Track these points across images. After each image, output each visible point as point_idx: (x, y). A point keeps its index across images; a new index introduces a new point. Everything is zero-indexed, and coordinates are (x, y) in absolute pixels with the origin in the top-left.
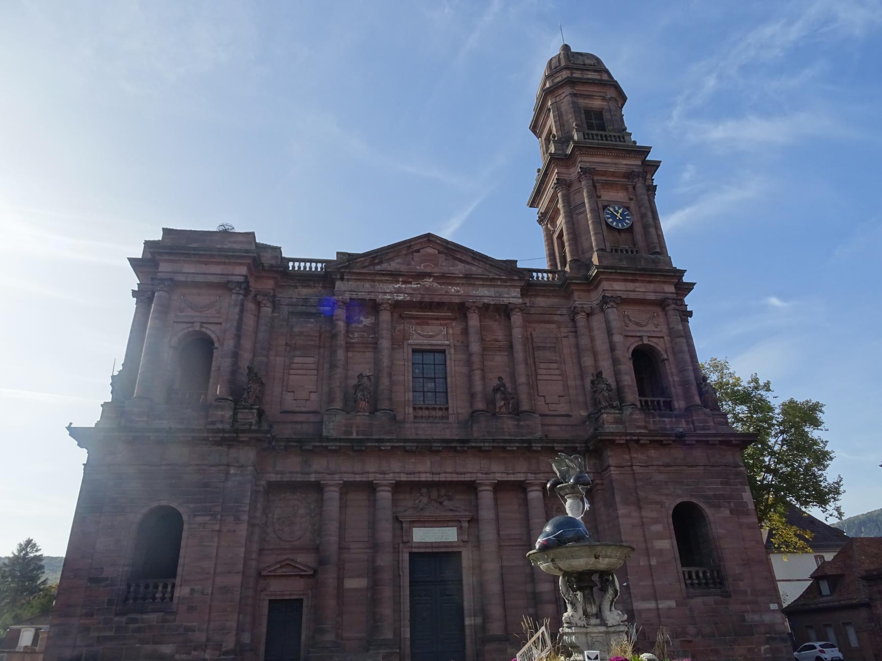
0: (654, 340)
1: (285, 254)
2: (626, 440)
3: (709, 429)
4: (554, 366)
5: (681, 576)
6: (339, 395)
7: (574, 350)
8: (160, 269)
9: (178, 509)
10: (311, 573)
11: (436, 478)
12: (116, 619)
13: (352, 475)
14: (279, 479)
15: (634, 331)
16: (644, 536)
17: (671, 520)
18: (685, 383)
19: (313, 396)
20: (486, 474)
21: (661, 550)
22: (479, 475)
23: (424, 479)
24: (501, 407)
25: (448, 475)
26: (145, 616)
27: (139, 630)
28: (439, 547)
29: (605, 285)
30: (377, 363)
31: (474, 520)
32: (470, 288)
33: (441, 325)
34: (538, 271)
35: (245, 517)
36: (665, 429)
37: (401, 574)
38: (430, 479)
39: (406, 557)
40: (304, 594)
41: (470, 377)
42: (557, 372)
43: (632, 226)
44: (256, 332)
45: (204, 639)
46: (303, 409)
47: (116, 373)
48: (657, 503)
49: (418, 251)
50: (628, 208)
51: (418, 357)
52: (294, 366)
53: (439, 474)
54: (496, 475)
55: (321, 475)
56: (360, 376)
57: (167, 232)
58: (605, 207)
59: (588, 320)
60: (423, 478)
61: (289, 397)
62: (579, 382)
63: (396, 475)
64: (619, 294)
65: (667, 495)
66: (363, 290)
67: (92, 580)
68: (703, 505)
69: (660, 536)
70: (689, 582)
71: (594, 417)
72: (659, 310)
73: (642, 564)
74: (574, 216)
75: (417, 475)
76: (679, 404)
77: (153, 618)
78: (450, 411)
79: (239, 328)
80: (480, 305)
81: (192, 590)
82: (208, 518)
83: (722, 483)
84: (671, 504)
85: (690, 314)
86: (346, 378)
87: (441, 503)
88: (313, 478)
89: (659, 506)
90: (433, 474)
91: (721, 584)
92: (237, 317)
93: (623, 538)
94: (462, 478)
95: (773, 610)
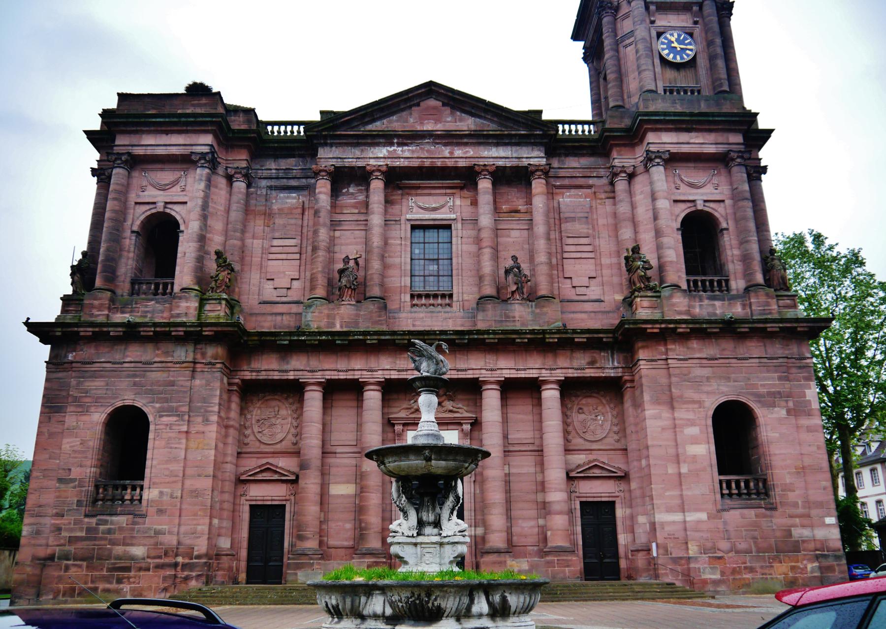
0: (712, 205)
1: (262, 116)
2: (660, 328)
3: (770, 313)
5: (717, 486)
6: (321, 281)
7: (611, 221)
8: (117, 143)
10: (294, 478)
12: (86, 520)
13: (336, 373)
14: (254, 377)
16: (676, 441)
17: (710, 422)
18: (746, 259)
19: (296, 284)
20: (492, 370)
21: (694, 457)
22: (483, 372)
24: (513, 293)
26: (114, 518)
27: (109, 531)
29: (651, 137)
30: (367, 242)
31: (476, 424)
32: (482, 148)
33: (446, 194)
34: (563, 122)
35: (215, 418)
36: (715, 314)
40: (286, 500)
41: (478, 255)
42: (589, 248)
43: (695, 57)
44: (228, 211)
45: (175, 543)
47: (75, 263)
48: (694, 402)
49: (418, 105)
50: (691, 35)
51: (419, 234)
52: (274, 250)
54: (504, 371)
55: (300, 373)
56: (346, 260)
57: (122, 97)
58: (659, 35)
59: (629, 183)
61: (269, 286)
63: (386, 372)
64: (668, 147)
65: (708, 393)
67: (60, 480)
68: (752, 405)
69: (695, 441)
70: (726, 491)
71: (629, 302)
72: (721, 167)
73: (670, 471)
74: (621, 49)
76: (737, 284)
77: (122, 520)
78: (455, 298)
79: (205, 206)
81: (161, 493)
82: (175, 419)
83: (780, 378)
84: (711, 403)
85: (764, 170)
86: (331, 261)
88: (291, 376)
89: (696, 406)
91: (767, 494)
92: (202, 194)
93: (650, 443)
94: (462, 375)
95: (829, 525)
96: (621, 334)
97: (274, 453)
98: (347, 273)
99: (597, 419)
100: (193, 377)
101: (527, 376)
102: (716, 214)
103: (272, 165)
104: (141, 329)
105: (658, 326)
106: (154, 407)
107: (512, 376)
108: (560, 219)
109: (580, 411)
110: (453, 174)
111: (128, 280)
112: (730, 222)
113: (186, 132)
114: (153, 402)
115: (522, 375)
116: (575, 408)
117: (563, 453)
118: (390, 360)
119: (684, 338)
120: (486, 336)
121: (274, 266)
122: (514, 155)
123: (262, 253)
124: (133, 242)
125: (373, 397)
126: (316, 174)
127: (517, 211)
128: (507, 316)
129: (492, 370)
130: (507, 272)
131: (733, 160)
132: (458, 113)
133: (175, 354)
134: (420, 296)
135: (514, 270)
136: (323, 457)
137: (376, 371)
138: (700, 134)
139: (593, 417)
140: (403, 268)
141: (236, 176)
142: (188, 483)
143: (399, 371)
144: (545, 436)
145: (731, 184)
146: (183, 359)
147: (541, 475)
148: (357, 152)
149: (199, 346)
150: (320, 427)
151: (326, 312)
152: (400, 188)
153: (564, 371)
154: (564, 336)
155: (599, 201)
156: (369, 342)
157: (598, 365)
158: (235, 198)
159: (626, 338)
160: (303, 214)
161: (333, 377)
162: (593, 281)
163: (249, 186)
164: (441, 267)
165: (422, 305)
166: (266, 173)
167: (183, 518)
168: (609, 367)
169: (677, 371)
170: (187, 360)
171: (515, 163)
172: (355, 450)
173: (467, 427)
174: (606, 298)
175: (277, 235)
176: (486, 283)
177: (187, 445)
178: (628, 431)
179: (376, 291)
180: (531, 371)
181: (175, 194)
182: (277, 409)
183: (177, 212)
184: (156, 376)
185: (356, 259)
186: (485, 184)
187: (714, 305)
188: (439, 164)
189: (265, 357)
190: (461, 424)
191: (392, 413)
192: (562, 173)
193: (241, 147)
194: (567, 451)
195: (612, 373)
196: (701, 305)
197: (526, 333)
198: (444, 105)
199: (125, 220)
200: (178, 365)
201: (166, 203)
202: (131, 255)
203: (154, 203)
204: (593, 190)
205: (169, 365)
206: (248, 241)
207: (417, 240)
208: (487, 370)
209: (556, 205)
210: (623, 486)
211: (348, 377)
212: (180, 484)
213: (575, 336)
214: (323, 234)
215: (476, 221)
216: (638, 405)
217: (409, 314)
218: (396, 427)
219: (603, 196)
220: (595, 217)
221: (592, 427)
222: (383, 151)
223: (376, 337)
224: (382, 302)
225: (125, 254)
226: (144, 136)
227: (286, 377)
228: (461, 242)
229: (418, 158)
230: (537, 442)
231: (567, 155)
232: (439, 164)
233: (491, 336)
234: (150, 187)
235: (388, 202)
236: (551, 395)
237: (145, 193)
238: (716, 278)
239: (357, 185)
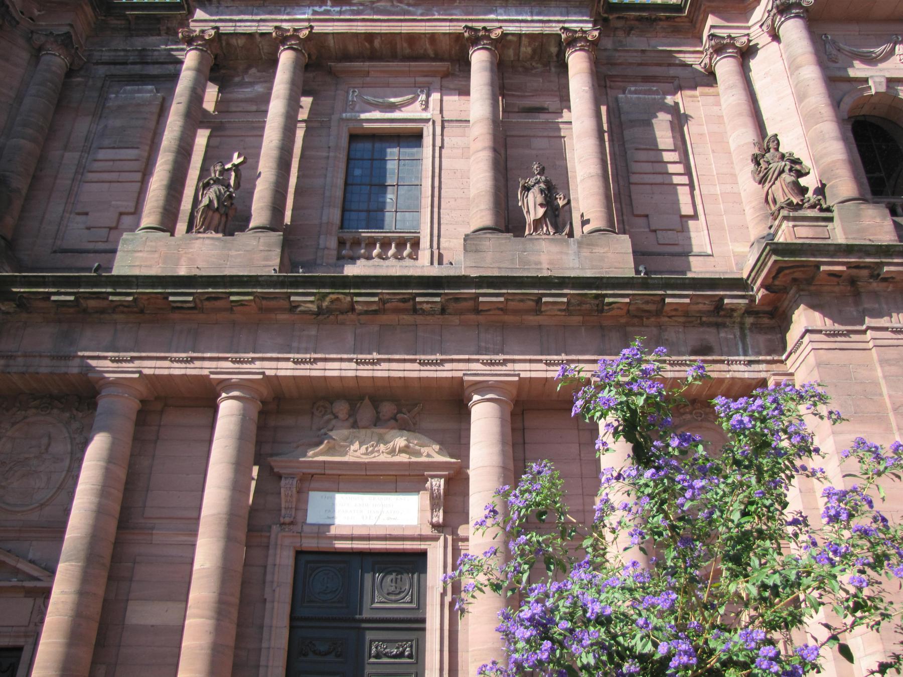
28: (369, 538)
37: (268, 596)
96: (763, 285)
107: (534, 375)
123: (76, 172)
140: (327, 194)
163: (70, 73)
166: (107, 56)
182: (45, 441)
207: (359, 155)
218: (283, 482)
227: (63, 370)
231: (629, 31)
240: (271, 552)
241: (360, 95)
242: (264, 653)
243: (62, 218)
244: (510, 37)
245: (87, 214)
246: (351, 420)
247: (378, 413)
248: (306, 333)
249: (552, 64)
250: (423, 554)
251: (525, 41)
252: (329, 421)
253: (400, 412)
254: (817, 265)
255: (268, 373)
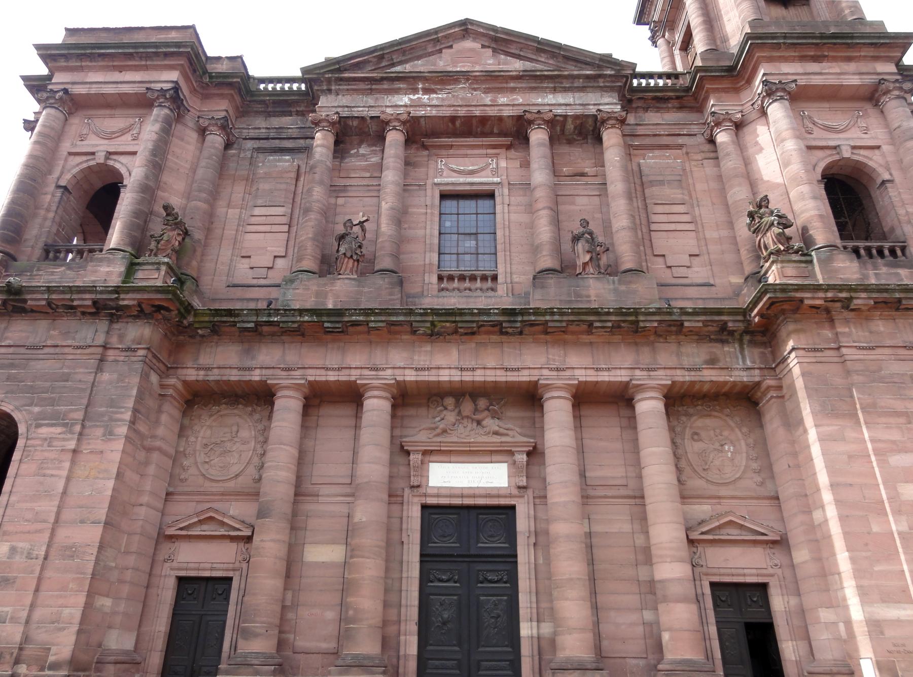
0: (862, 152)
4: (681, 209)
7: (714, 185)
9: (12, 414)
11: (468, 377)
13: (323, 372)
14: (200, 378)
15: (821, 139)
19: (280, 263)
20: (558, 370)
22: (546, 372)
23: (447, 379)
24: (585, 265)
25: (488, 372)
28: (474, 496)
31: (535, 453)
33: (487, 155)
35: (123, 430)
37: (405, 539)
38: (457, 379)
39: (414, 514)
44: (194, 170)
45: (18, 638)
46: (262, 282)
49: (451, 47)
51: (451, 205)
52: (254, 220)
53: (473, 369)
54: (577, 372)
55: (270, 372)
59: (737, 135)
60: (445, 376)
61: (244, 265)
62: (725, 233)
63: (397, 372)
66: (362, 105)
72: (868, 106)
75: (433, 372)
78: (500, 279)
80: (548, 116)
81: (13, 550)
82: (59, 430)
87: (479, 423)
88: (256, 376)
90: (462, 369)
94: (512, 377)
96: (760, 314)
97: (222, 494)
98: (348, 239)
99: (725, 447)
100: (99, 369)
101: (612, 379)
102: (871, 163)
103: (261, 124)
104: (29, 297)
105: (821, 295)
106: (30, 412)
107: (589, 379)
108: (642, 184)
109: (696, 436)
110: (496, 131)
111: (41, 245)
112: (893, 172)
113: (146, 68)
114: (30, 405)
115: (605, 377)
116: (688, 432)
117: (679, 499)
118: (405, 354)
119: (861, 315)
120: (548, 318)
121: (251, 240)
122: (577, 102)
123: (239, 225)
124: (57, 199)
125: (376, 407)
126: (316, 123)
127: (583, 175)
128: (578, 295)
129: (558, 370)
130: (576, 239)
131: (887, 92)
132: (502, 57)
133: (78, 336)
134: (451, 278)
135: (584, 235)
136: (295, 502)
137: (383, 369)
138: (834, 64)
139: (717, 445)
140: (428, 242)
141: (211, 128)
142: (63, 534)
143: (417, 369)
144: (645, 472)
145: (887, 126)
146: (89, 342)
147: (642, 537)
148: (370, 101)
149: (116, 326)
150: (295, 452)
151: (315, 288)
152: (425, 147)
153: (669, 372)
154: (667, 318)
155: (693, 163)
156: (372, 325)
157: (721, 365)
158: (205, 153)
159: (762, 324)
160: (297, 179)
161: (318, 379)
162: (696, 260)
163: (228, 145)
164: (480, 244)
165: (454, 289)
166: (253, 133)
167: (42, 594)
168: (738, 366)
169: (859, 366)
170: (95, 343)
171: (579, 111)
172: (348, 490)
173: (522, 458)
174: (718, 281)
175: (259, 202)
176: (544, 253)
177: (70, 470)
178: (777, 468)
179: (385, 262)
180: (618, 372)
181: (124, 143)
182: (235, 429)
183: (120, 164)
184: (45, 366)
185: (361, 223)
186: (538, 136)
187: (898, 274)
188: (477, 113)
189: (220, 349)
190: (511, 453)
191: (406, 436)
192: (640, 130)
193: (222, 96)
194: (684, 497)
195: (744, 377)
196: (876, 274)
197: (608, 314)
198: (483, 46)
199: (50, 172)
200: (79, 351)
201: (110, 153)
202: (51, 215)
203: (93, 154)
204: (684, 150)
205: (66, 350)
206: (221, 210)
208: (551, 369)
209: (635, 168)
210: (778, 557)
211: (341, 378)
212: (47, 535)
213: (684, 318)
214: (318, 193)
215: (527, 187)
216: (793, 423)
217: (436, 300)
218: (412, 457)
219: (699, 157)
220: (690, 181)
221: (717, 463)
222: (405, 99)
223: (383, 318)
224: (398, 276)
225: (42, 212)
226: (90, 74)
227: (248, 378)
228: (507, 211)
229: (450, 106)
230: (632, 483)
231: (646, 109)
232: (478, 113)
233: (556, 318)
234: (93, 136)
235: (408, 163)
236: (649, 407)
237: (83, 143)
238: (887, 245)
239: (369, 146)
240: (405, 507)
241: (445, 165)
242: (404, 581)
243: (231, 260)
244: (558, 118)
245: (249, 257)
246: (457, 411)
247: (476, 405)
248: (423, 349)
249: (589, 137)
250: (513, 508)
251: (570, 120)
252: (441, 411)
253: (491, 404)
254: (801, 300)
255: (399, 378)
